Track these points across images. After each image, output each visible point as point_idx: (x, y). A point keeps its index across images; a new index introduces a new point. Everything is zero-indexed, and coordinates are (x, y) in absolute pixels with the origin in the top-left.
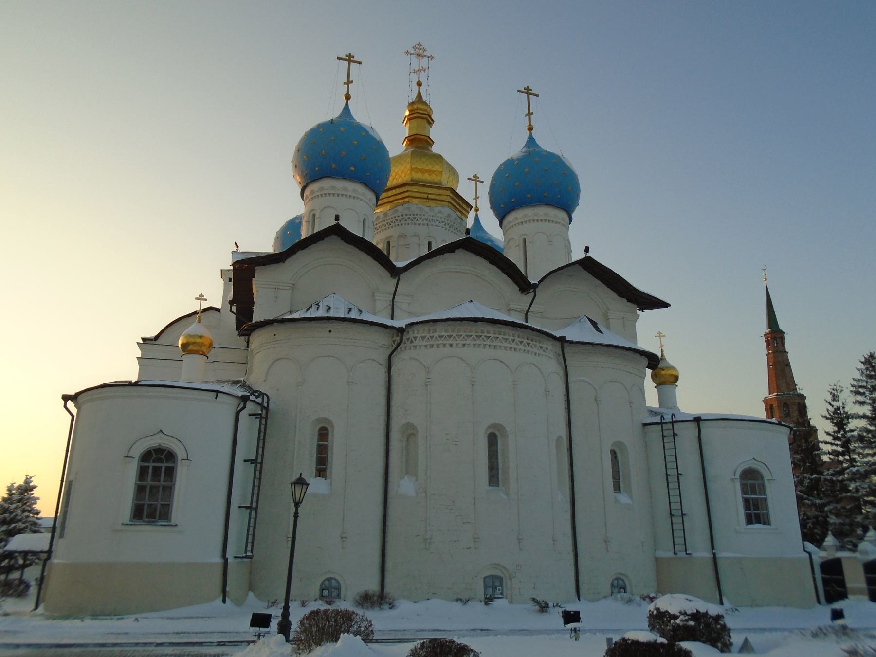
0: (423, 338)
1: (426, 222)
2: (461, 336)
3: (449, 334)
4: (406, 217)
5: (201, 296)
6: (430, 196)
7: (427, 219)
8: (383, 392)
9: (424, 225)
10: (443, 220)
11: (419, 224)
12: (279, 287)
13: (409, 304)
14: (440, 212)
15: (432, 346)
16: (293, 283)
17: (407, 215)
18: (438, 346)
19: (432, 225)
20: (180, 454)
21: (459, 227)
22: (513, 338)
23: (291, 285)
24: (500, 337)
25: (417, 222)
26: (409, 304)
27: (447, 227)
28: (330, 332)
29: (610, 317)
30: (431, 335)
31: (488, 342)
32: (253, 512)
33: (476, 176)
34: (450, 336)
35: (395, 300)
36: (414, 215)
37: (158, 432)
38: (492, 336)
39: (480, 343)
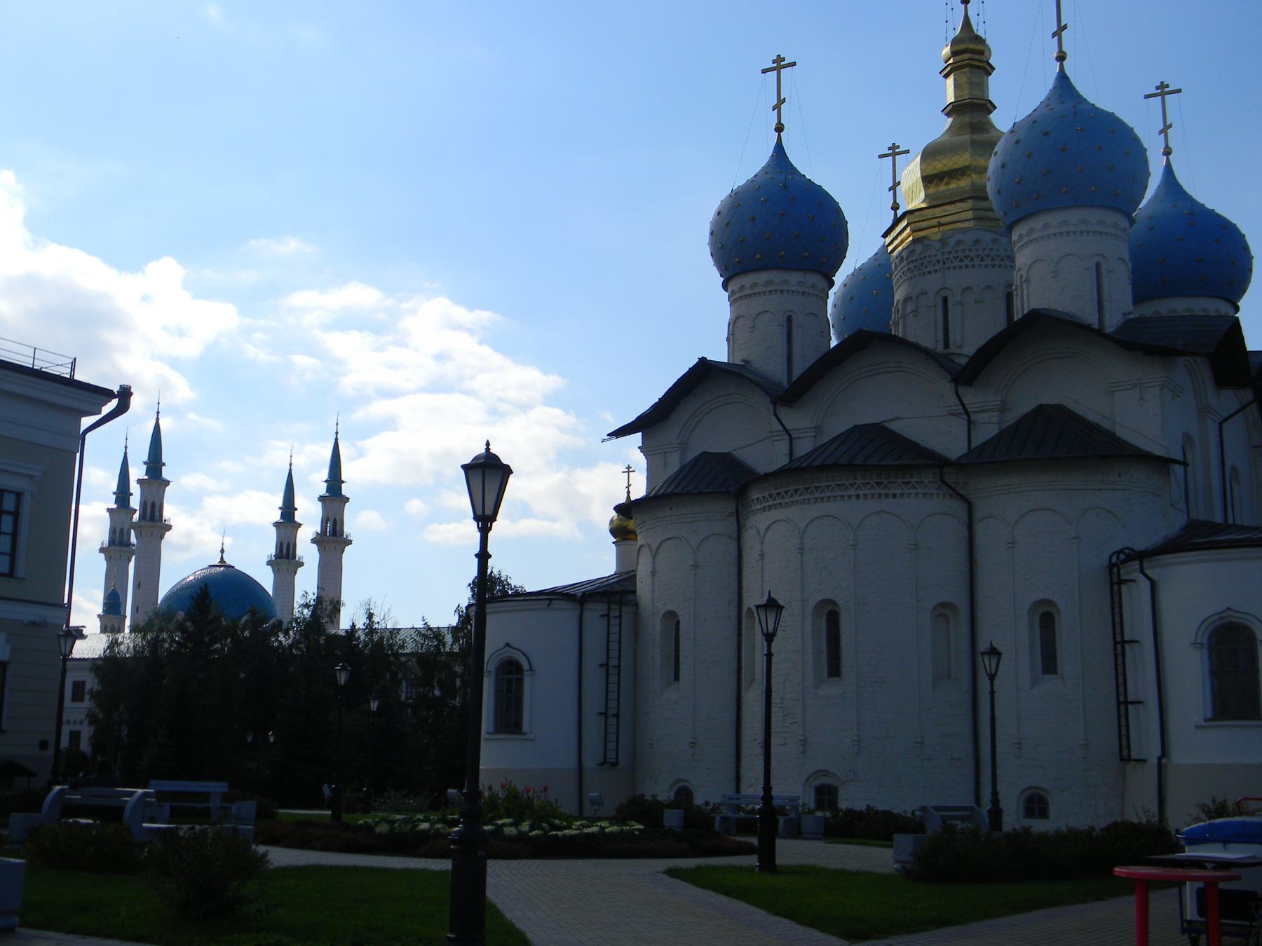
0: (758, 499)
1: (937, 267)
2: (789, 491)
3: (777, 491)
4: (911, 266)
5: (629, 467)
6: (943, 220)
7: (938, 261)
8: (735, 571)
9: (936, 271)
10: (967, 253)
11: (930, 272)
12: (666, 450)
13: (815, 437)
14: (959, 242)
15: (764, 507)
16: (678, 442)
17: (912, 262)
18: (770, 507)
19: (949, 268)
20: (526, 667)
21: (1006, 250)
22: (851, 482)
23: (676, 446)
24: (833, 484)
25: (926, 270)
26: (815, 437)
27: (977, 262)
28: (671, 509)
29: (1112, 389)
30: (763, 495)
31: (817, 495)
32: (612, 721)
33: (1162, 86)
34: (778, 494)
35: (793, 436)
36: (921, 259)
37: (505, 647)
38: (823, 484)
39: (810, 496)
